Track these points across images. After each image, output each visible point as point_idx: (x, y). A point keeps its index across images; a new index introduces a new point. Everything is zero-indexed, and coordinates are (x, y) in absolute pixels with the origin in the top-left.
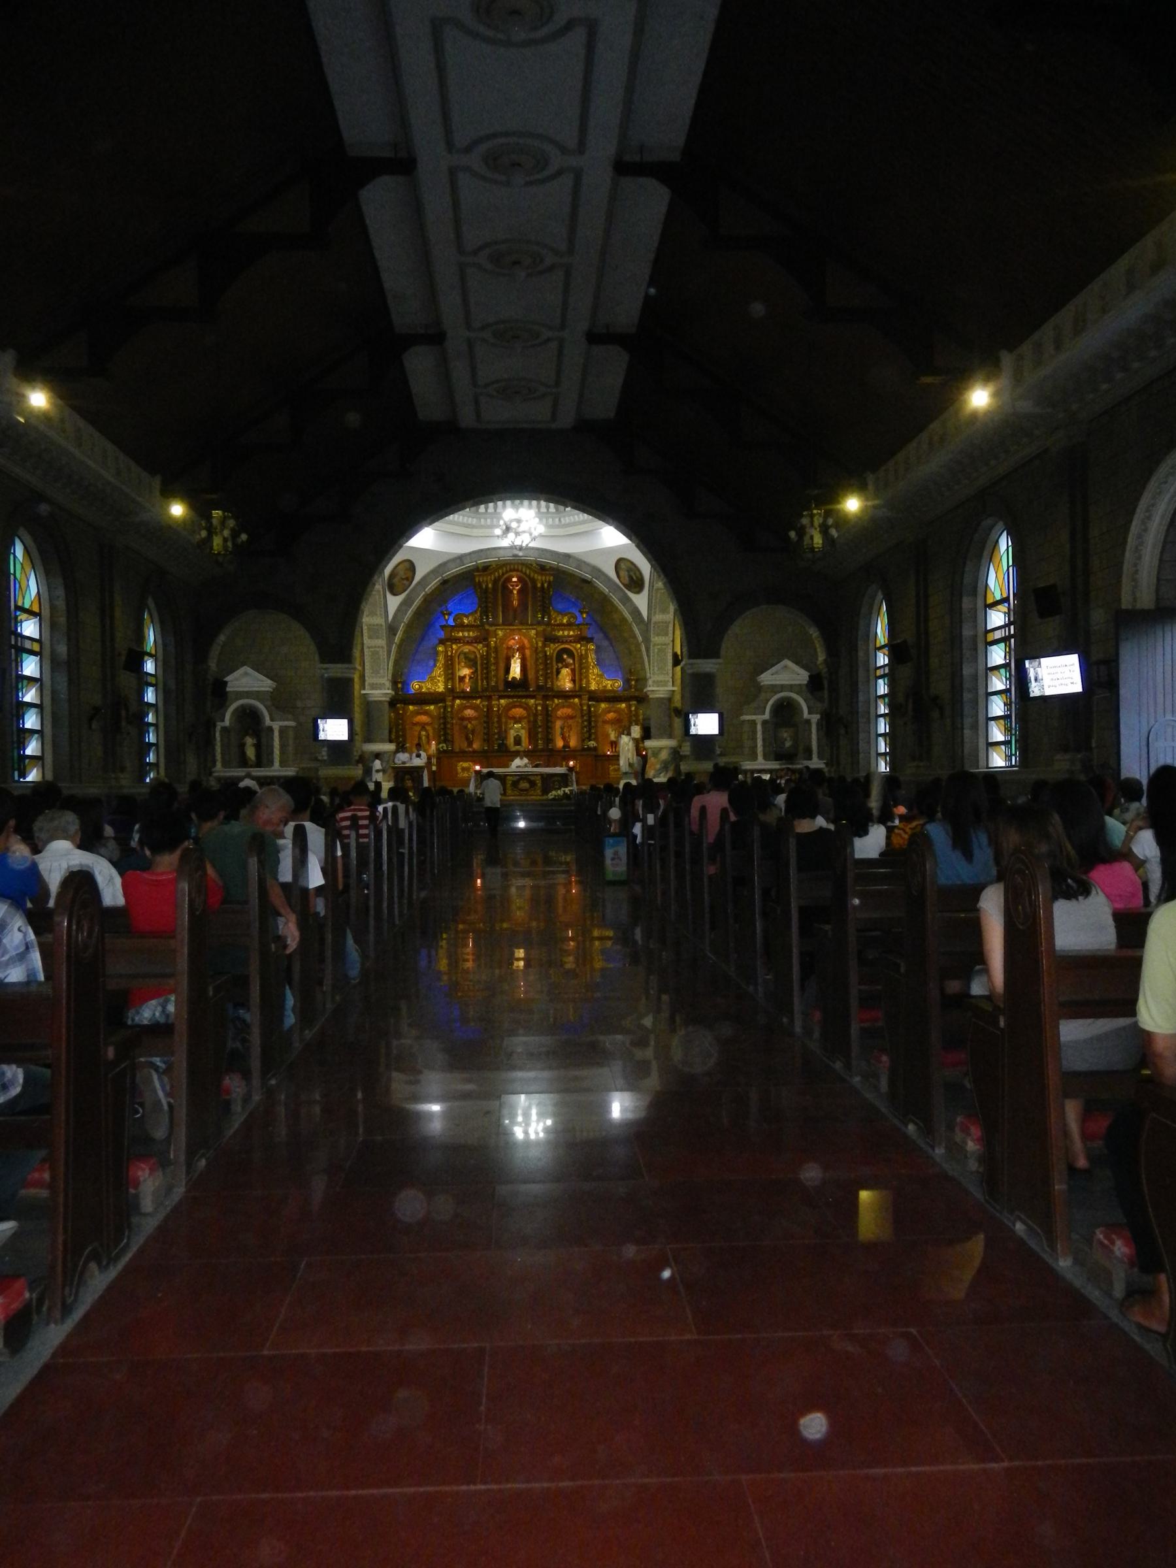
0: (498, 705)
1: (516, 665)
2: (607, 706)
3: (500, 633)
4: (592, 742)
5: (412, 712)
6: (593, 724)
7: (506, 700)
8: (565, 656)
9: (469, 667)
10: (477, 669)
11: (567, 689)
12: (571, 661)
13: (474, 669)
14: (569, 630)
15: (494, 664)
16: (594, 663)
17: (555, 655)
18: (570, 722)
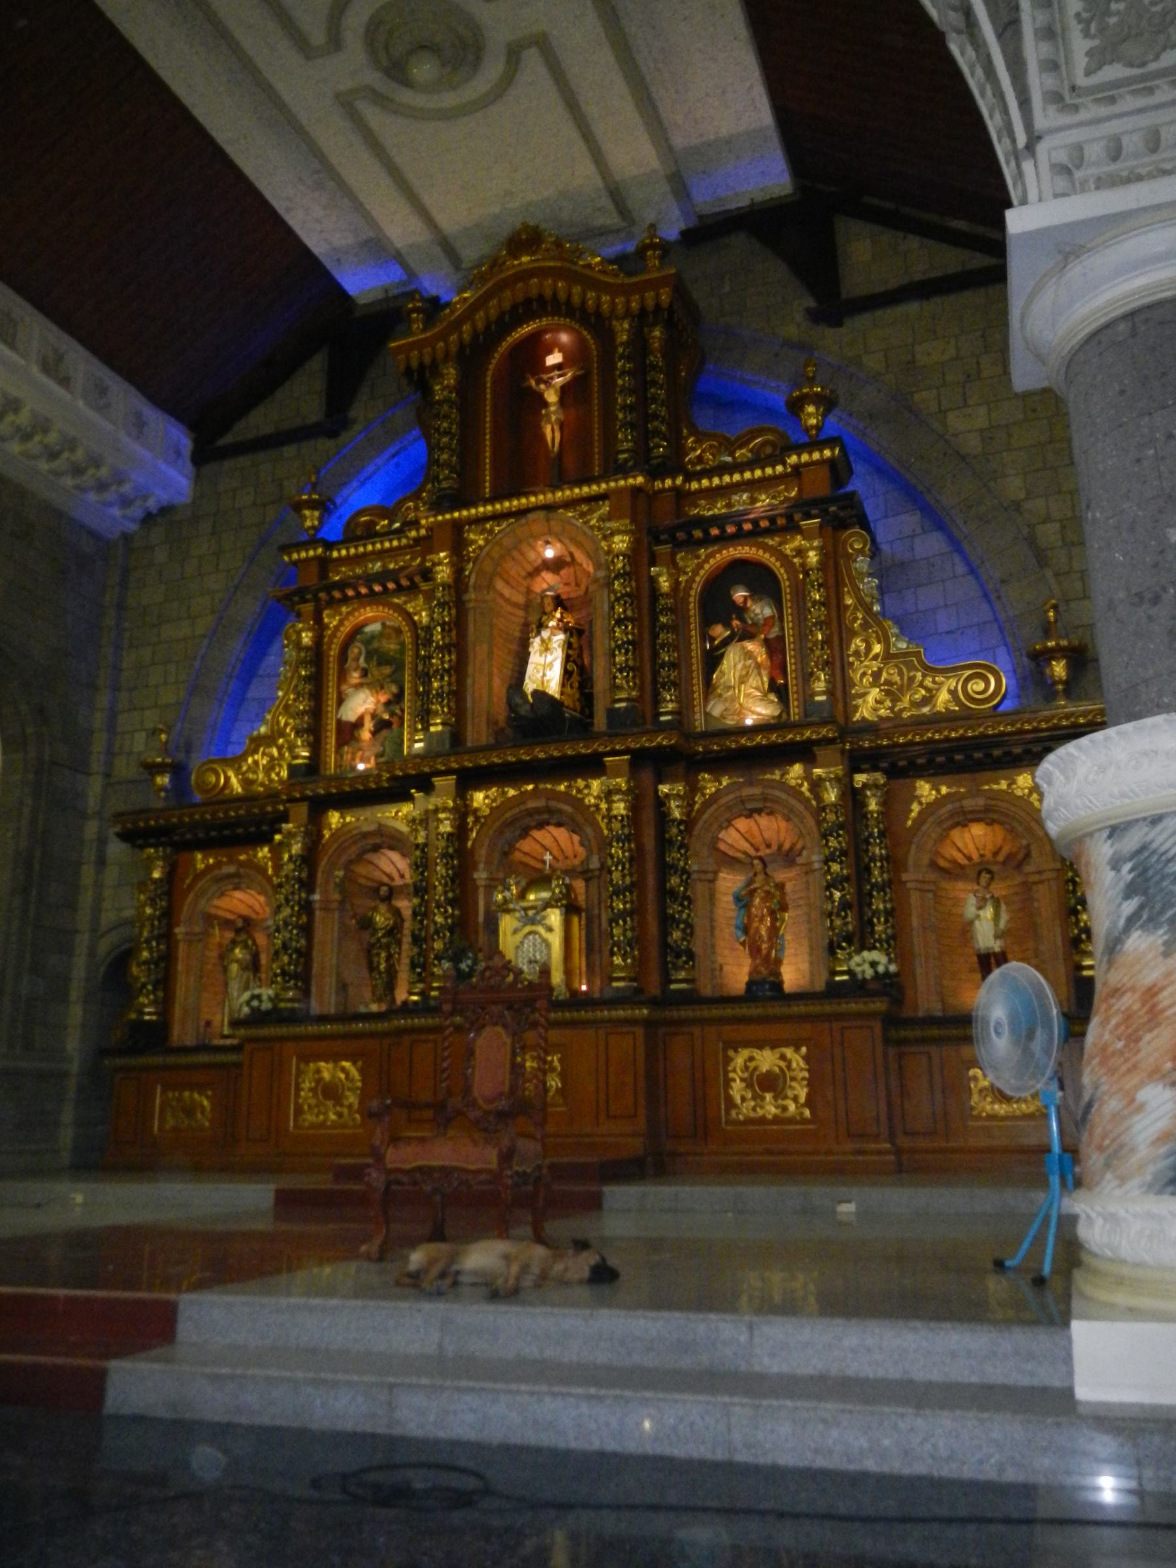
0: (463, 812)
1: (549, 658)
2: (944, 790)
3: (477, 539)
4: (875, 955)
5: (199, 876)
6: (877, 876)
8: (740, 595)
10: (398, 697)
11: (749, 722)
12: (768, 612)
14: (752, 486)
15: (445, 648)
16: (868, 610)
17: (697, 588)
18: (781, 875)
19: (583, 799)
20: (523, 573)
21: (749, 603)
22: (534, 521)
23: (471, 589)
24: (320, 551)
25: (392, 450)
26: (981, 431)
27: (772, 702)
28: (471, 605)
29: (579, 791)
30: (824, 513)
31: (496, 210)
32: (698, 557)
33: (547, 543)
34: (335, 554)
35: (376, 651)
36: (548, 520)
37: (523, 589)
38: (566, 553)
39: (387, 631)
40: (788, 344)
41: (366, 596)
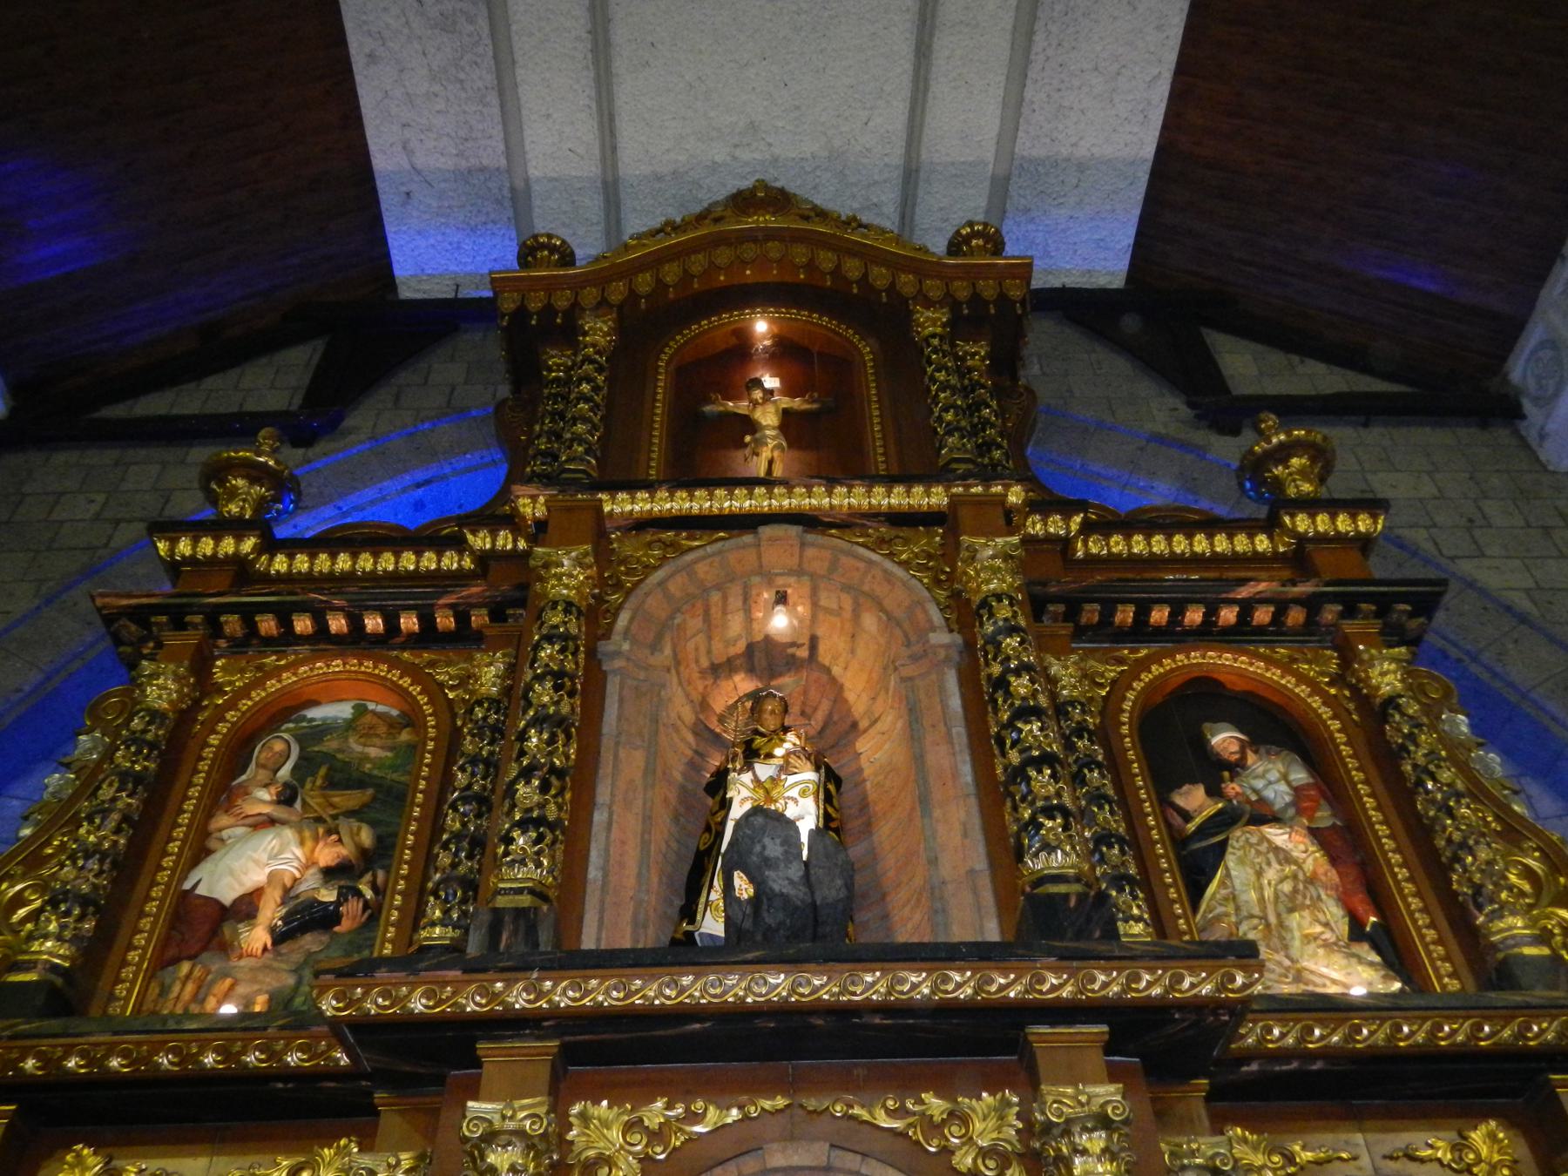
7: (656, 1112)
8: (1224, 739)
9: (324, 825)
12: (1300, 776)
13: (366, 837)
19: (947, 1151)
20: (705, 663)
21: (1251, 758)
22: (772, 540)
23: (616, 637)
24: (248, 545)
25: (421, 476)
26: (1527, 591)
27: (1371, 964)
28: (619, 663)
29: (933, 1127)
30: (1382, 613)
31: (719, 154)
32: (1120, 661)
33: (782, 599)
34: (280, 564)
35: (328, 757)
36: (803, 545)
37: (696, 697)
38: (805, 640)
39: (368, 719)
40: (1160, 439)
41: (338, 640)
